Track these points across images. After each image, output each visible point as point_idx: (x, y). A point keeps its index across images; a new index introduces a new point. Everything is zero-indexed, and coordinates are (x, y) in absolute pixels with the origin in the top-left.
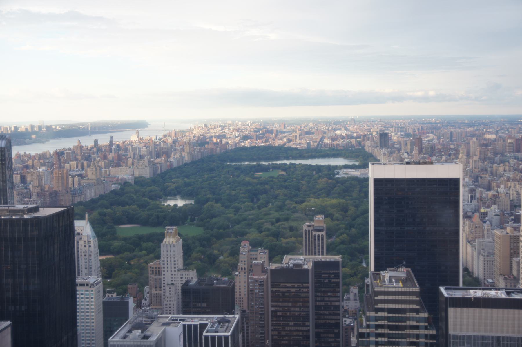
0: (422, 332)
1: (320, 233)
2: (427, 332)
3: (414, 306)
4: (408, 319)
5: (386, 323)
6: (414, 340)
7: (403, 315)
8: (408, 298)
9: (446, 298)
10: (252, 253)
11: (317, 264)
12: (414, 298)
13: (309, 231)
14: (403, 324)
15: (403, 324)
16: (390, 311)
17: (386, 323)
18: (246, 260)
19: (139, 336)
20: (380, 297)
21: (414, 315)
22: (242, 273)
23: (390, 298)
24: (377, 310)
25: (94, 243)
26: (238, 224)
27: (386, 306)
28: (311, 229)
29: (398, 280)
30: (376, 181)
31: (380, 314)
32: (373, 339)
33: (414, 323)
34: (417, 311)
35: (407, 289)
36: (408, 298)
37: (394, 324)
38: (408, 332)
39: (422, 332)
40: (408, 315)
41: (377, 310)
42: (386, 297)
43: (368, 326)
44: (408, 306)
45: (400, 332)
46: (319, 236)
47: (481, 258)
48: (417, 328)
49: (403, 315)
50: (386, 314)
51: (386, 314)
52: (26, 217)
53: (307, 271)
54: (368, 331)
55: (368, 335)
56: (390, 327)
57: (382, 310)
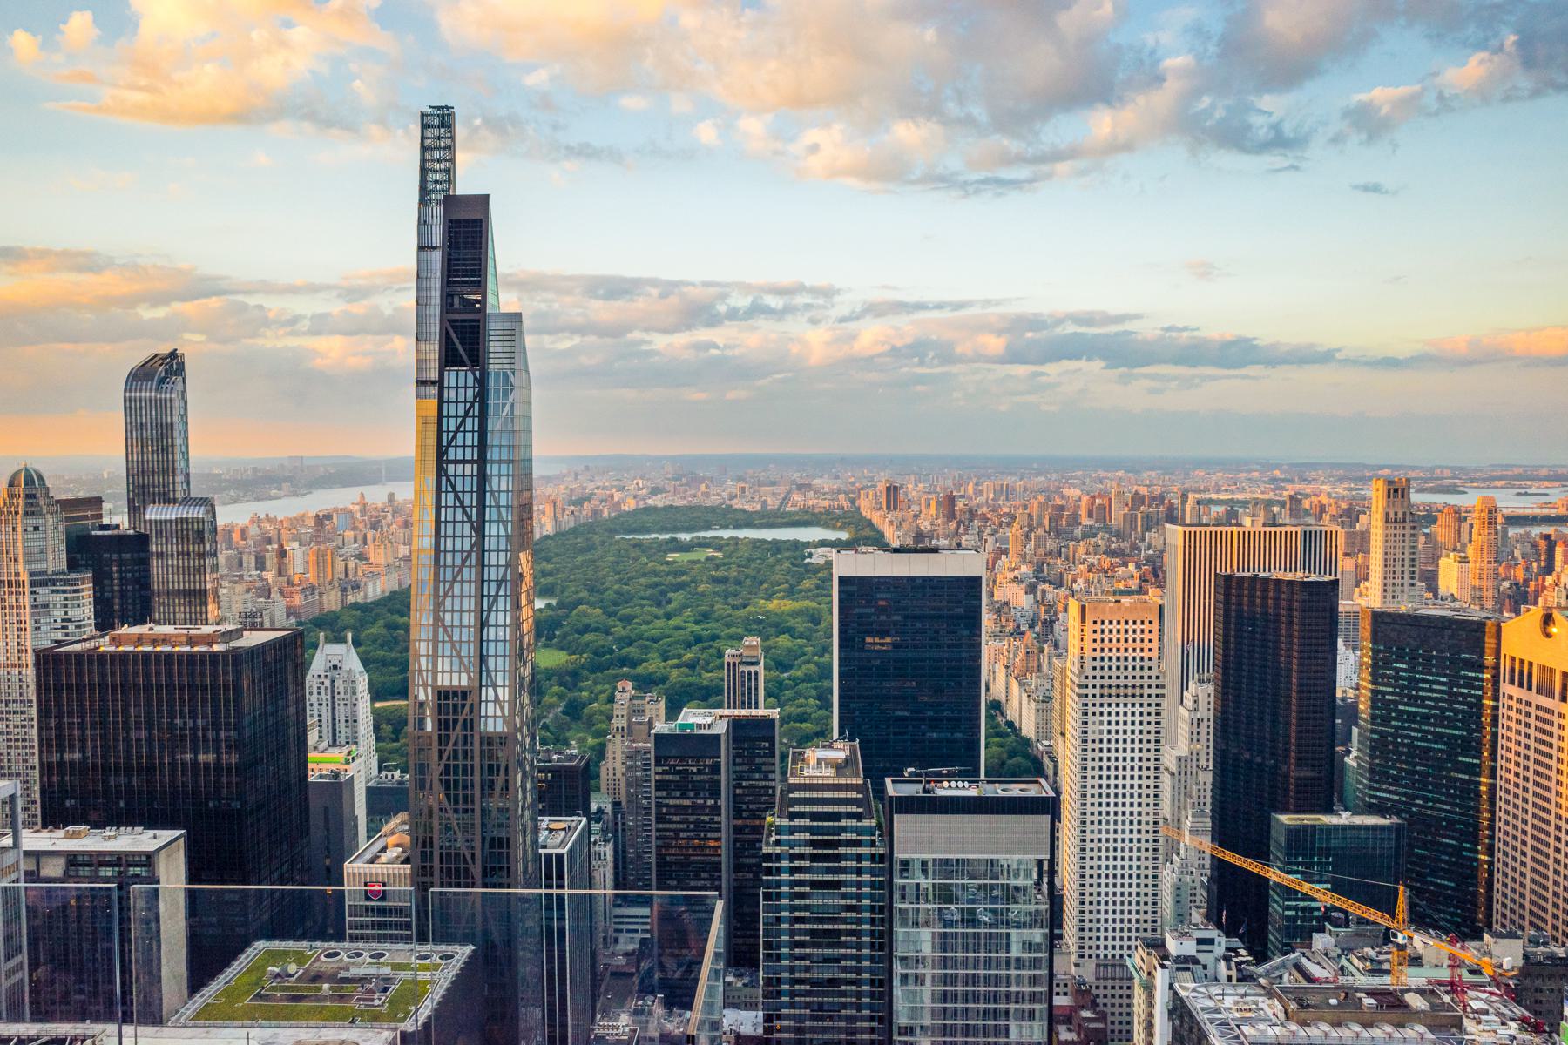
0: (866, 850)
1: (753, 669)
2: (874, 851)
3: (854, 809)
4: (844, 829)
5: (808, 836)
6: (854, 864)
7: (836, 824)
8: (843, 795)
9: (891, 797)
10: (636, 702)
11: (737, 725)
12: (854, 795)
13: (734, 664)
14: (836, 838)
15: (836, 838)
16: (815, 816)
17: (808, 836)
18: (625, 713)
19: (398, 857)
20: (797, 794)
21: (854, 823)
22: (618, 737)
23: (815, 795)
24: (793, 816)
25: (363, 683)
26: (630, 644)
27: (808, 808)
28: (737, 660)
29: (829, 763)
30: (843, 581)
31: (797, 822)
32: (785, 863)
33: (854, 837)
34: (858, 816)
35: (843, 781)
36: (843, 795)
37: (820, 838)
38: (843, 850)
39: (866, 850)
40: (844, 823)
41: (793, 816)
42: (808, 794)
43: (778, 843)
44: (844, 809)
45: (831, 852)
46: (749, 673)
47: (1033, 704)
48: (857, 844)
49: (836, 824)
50: (808, 822)
51: (808, 822)
52: (216, 648)
53: (718, 737)
54: (778, 850)
55: (778, 857)
56: (813, 844)
57: (801, 815)
